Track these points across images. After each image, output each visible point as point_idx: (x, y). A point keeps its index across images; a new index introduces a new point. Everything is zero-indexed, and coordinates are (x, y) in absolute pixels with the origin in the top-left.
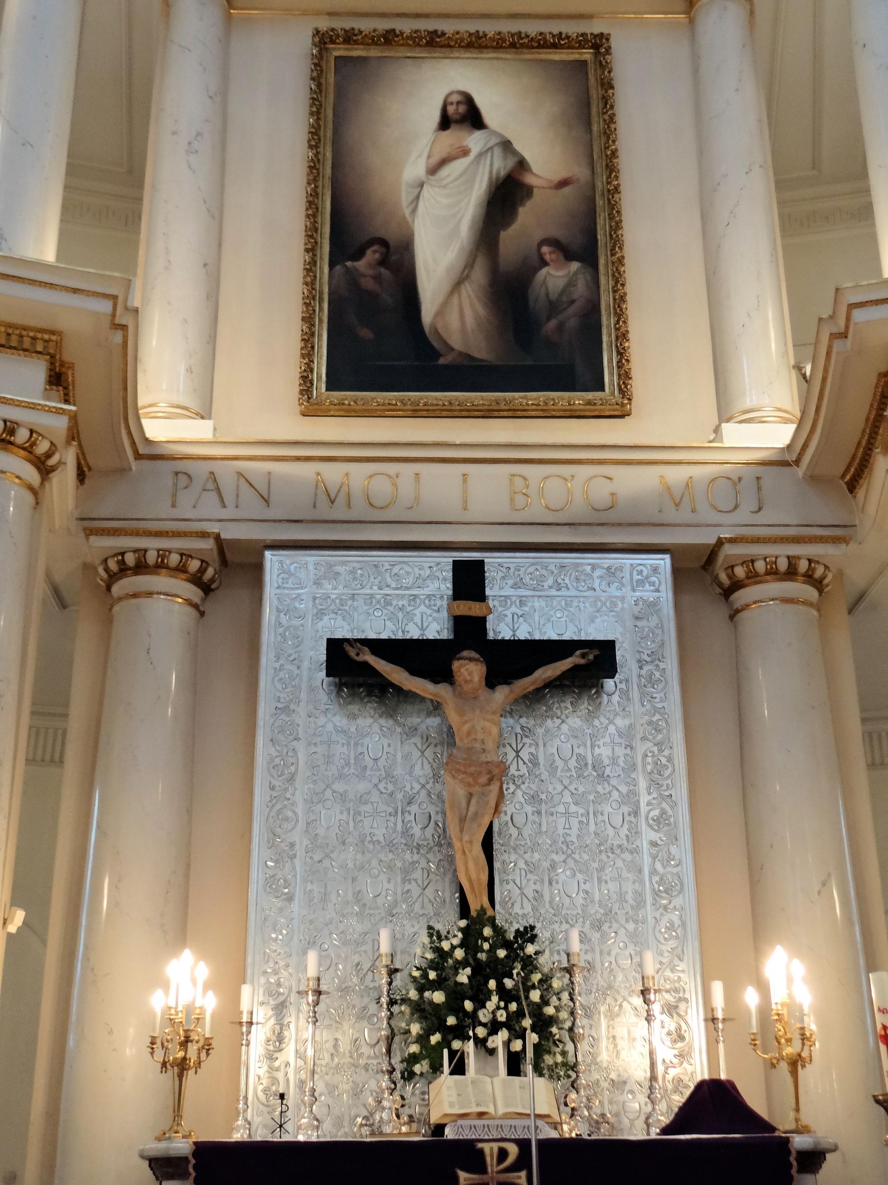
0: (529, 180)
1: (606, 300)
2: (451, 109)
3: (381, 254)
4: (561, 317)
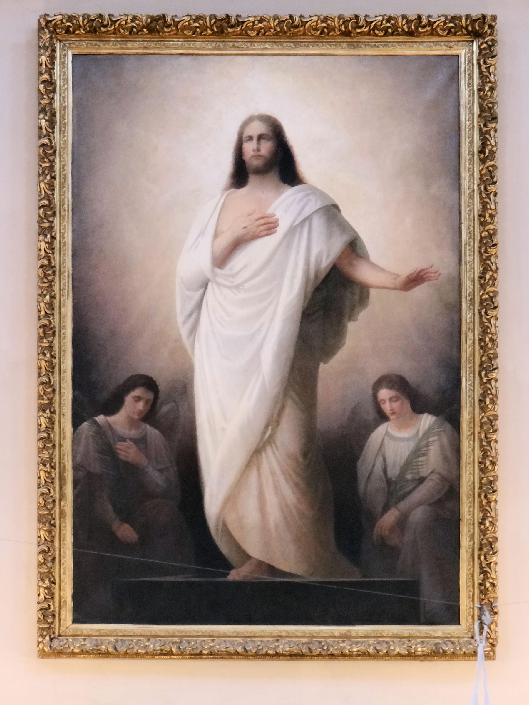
0: (363, 273)
1: (469, 478)
2: (249, 148)
3: (147, 402)
4: (403, 505)
